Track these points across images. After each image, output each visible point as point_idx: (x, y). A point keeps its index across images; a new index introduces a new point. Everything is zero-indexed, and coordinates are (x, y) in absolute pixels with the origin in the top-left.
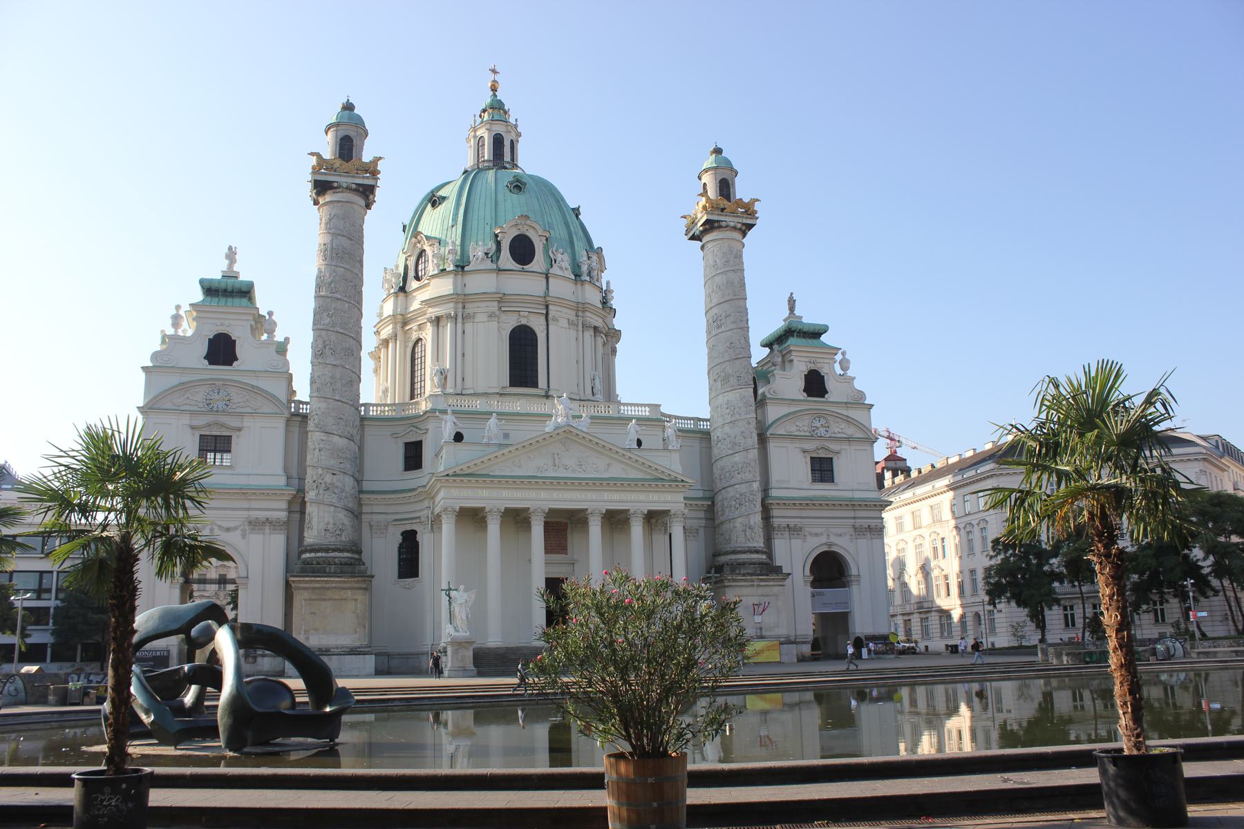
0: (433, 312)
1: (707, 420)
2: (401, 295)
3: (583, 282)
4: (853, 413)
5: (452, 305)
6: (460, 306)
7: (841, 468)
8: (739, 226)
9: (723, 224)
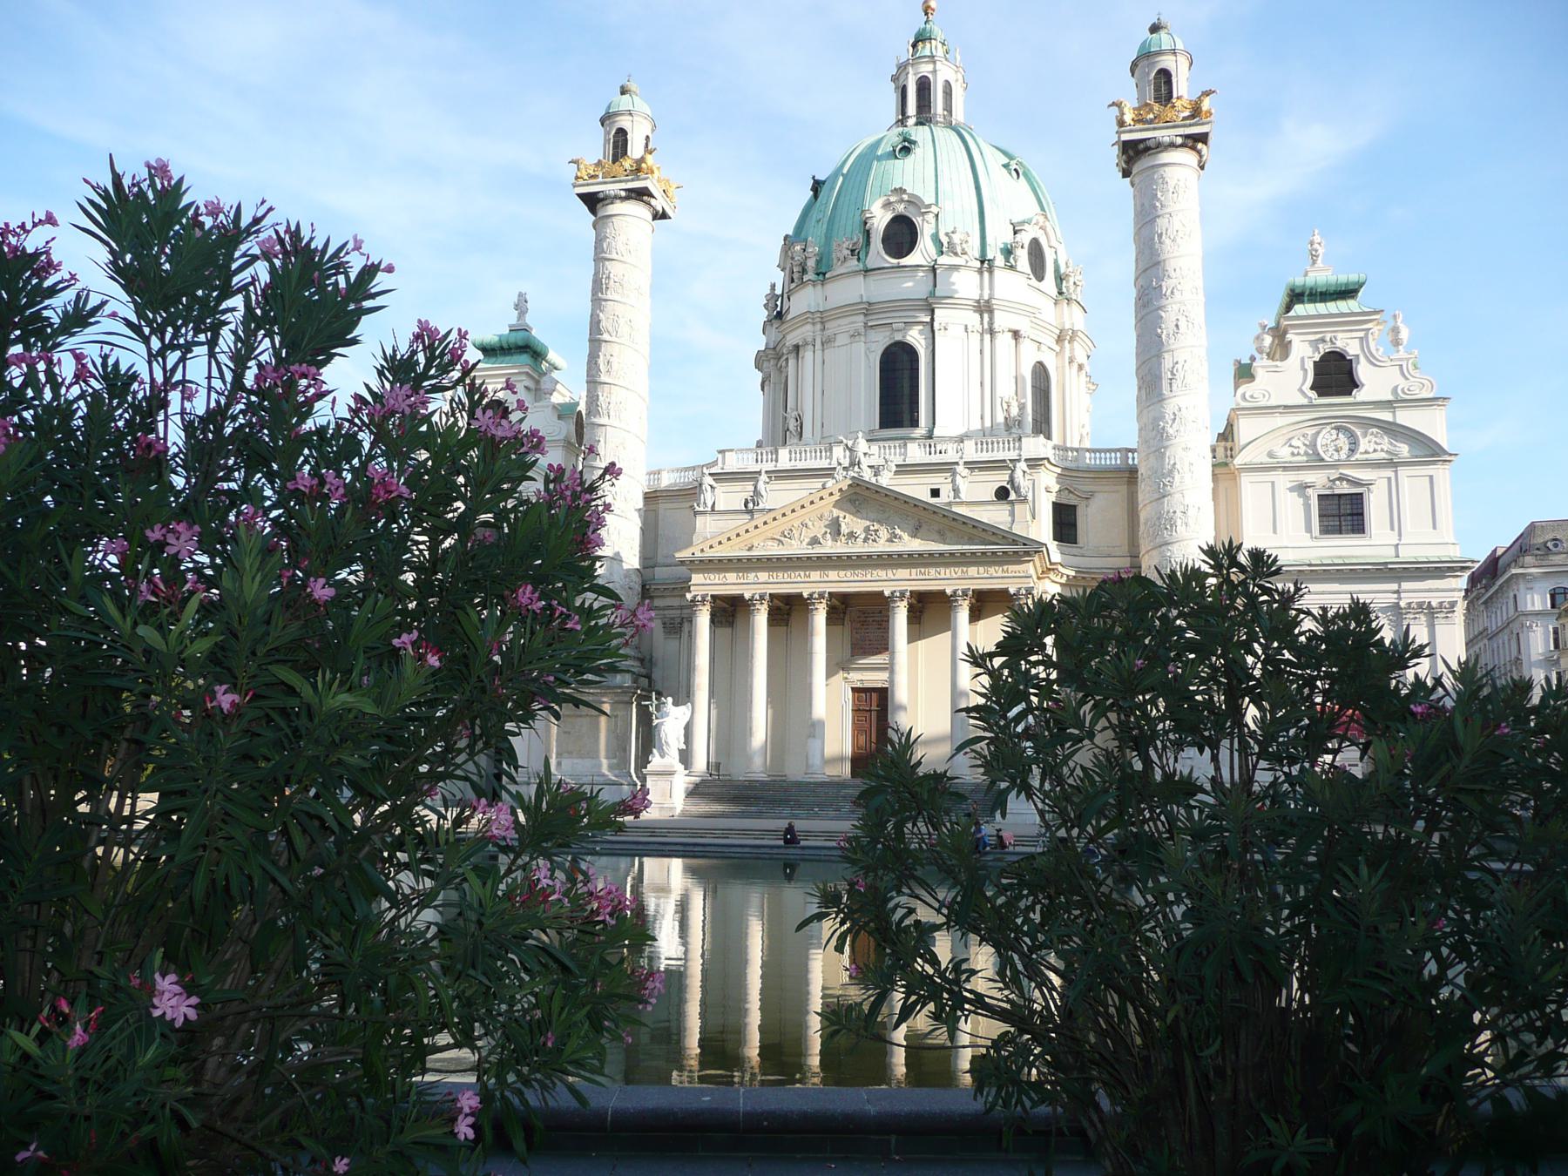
0: (792, 339)
1: (1133, 451)
2: (776, 323)
3: (991, 270)
4: (1405, 418)
5: (809, 327)
6: (819, 326)
7: (1376, 508)
8: (1179, 141)
9: (1149, 143)
